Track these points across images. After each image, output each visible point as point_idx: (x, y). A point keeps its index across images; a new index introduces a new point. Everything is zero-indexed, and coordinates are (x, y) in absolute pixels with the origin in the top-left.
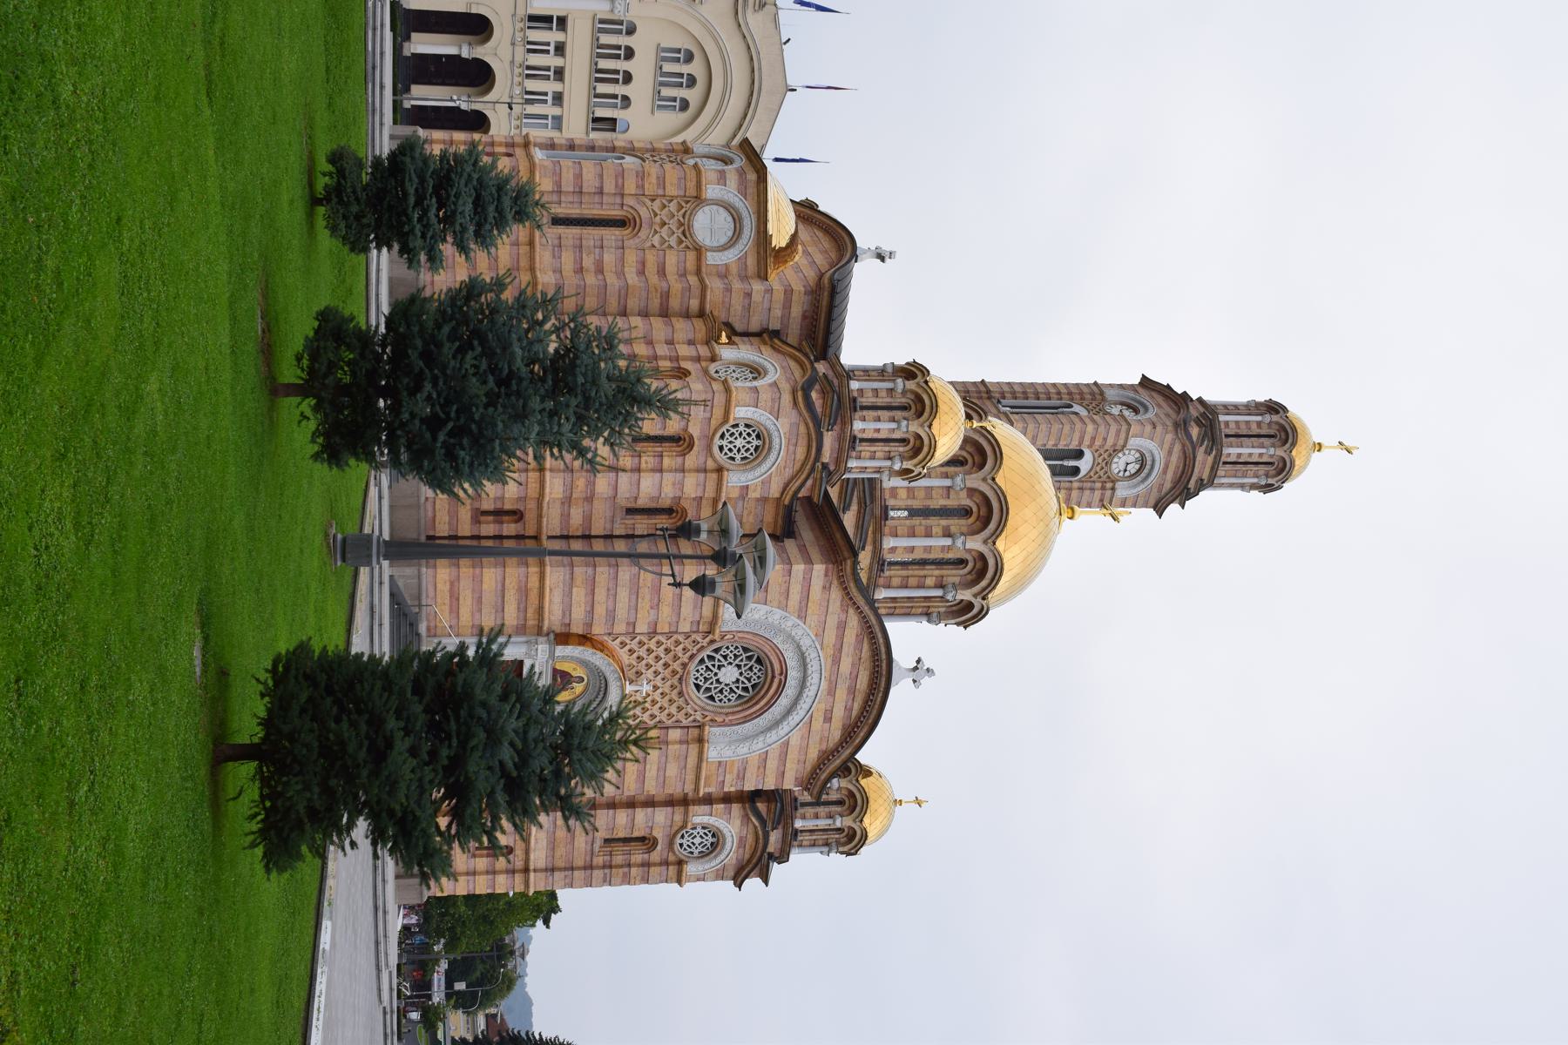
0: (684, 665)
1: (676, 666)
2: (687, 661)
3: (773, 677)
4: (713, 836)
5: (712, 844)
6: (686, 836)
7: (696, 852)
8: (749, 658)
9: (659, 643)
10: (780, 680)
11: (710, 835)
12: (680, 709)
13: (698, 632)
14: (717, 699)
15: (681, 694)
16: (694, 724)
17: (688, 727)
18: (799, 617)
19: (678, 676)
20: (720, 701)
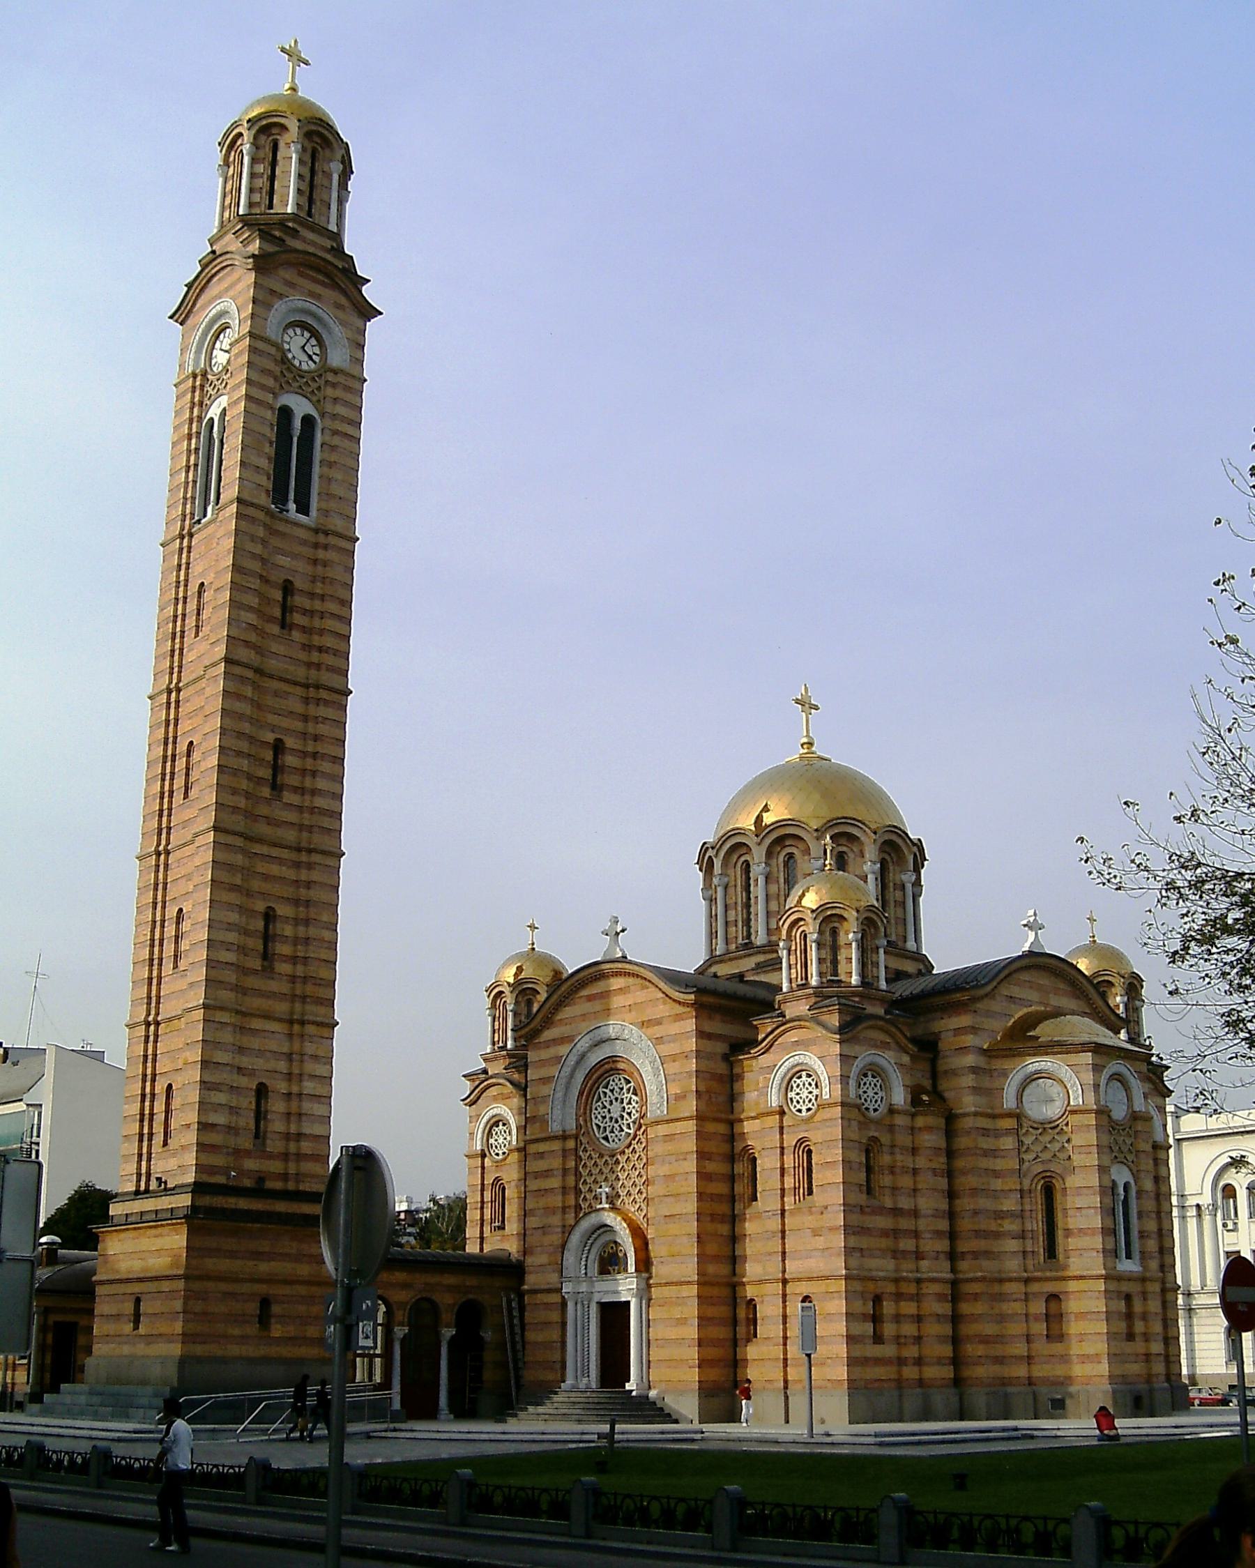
1: (601, 1162)
5: (809, 1076)
6: (798, 1107)
7: (816, 1092)
8: (605, 1094)
10: (614, 1062)
13: (576, 1149)
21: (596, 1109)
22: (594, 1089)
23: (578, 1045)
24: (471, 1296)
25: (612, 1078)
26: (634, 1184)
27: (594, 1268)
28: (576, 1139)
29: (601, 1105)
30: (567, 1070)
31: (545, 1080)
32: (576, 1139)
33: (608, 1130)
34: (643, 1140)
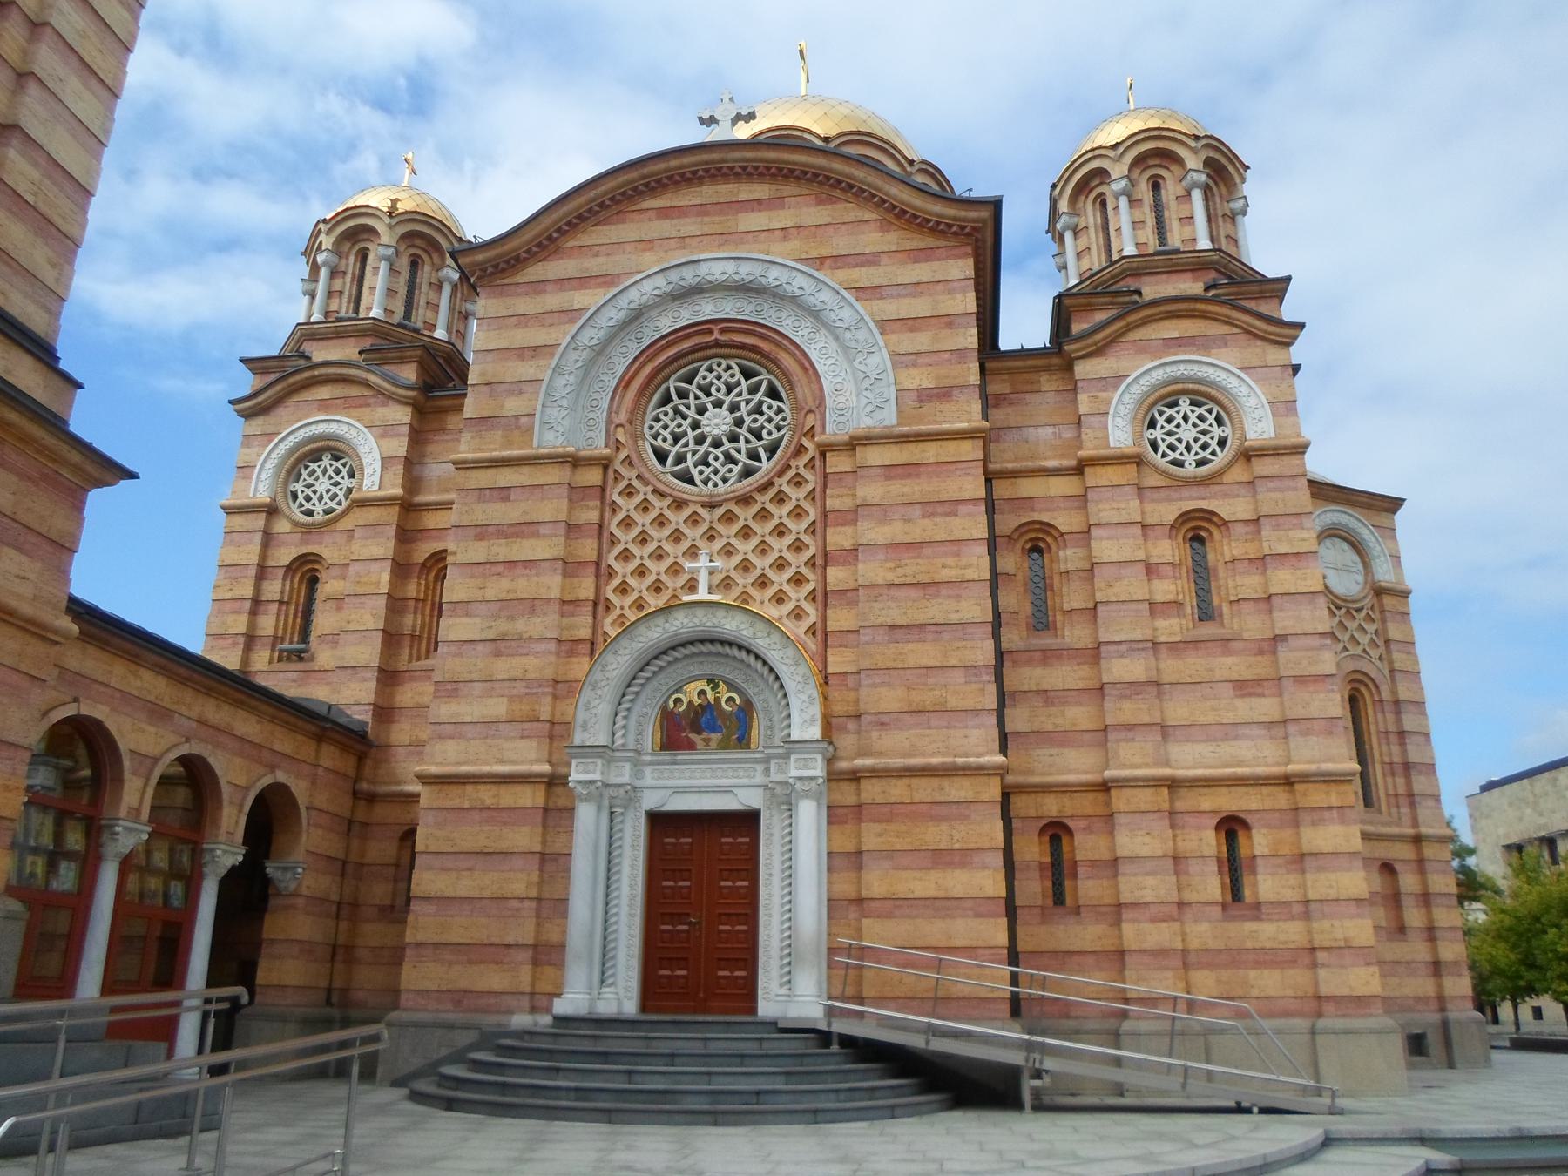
0: (679, 504)
1: (677, 519)
2: (669, 501)
3: (717, 344)
4: (1172, 405)
7: (1217, 432)
9: (626, 556)
10: (723, 331)
11: (1172, 412)
12: (780, 499)
13: (603, 489)
14: (776, 435)
15: (745, 500)
16: (818, 463)
17: (825, 476)
18: (572, 321)
19: (703, 512)
20: (779, 428)
21: (657, 420)
22: (659, 378)
23: (633, 294)
24: (281, 777)
25: (706, 364)
26: (780, 565)
27: (651, 736)
28: (606, 468)
29: (671, 412)
30: (592, 336)
31: (536, 351)
32: (606, 468)
33: (690, 461)
34: (808, 476)
